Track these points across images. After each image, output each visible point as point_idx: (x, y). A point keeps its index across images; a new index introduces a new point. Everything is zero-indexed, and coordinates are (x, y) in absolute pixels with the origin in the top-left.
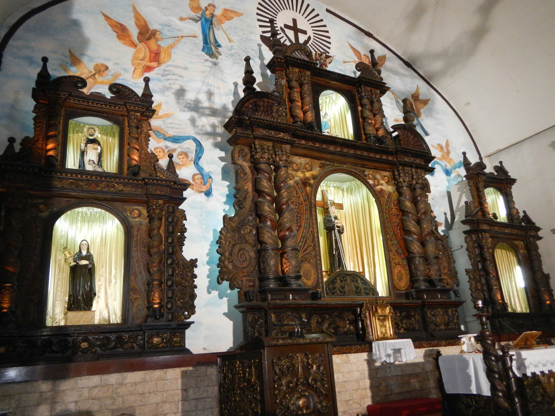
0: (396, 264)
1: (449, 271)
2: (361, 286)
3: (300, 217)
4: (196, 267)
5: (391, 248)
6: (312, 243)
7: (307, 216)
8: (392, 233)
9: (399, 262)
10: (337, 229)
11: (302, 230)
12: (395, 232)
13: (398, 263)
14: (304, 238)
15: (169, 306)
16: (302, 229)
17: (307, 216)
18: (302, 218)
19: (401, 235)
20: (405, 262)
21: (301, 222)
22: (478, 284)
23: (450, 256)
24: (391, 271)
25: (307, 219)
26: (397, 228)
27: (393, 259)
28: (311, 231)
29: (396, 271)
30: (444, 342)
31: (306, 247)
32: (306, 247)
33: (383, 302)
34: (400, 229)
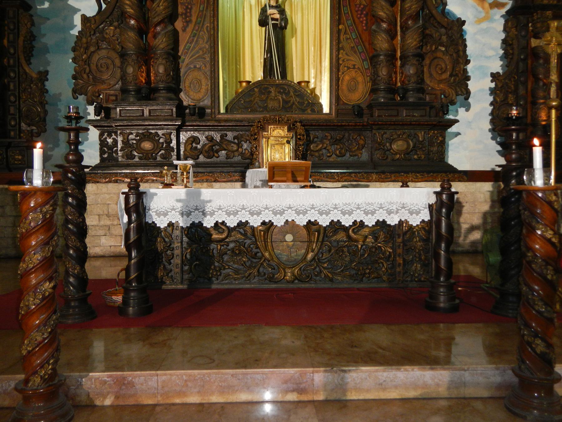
0: (349, 68)
1: (451, 76)
2: (294, 99)
3: (191, 9)
4: (47, 80)
5: (344, 44)
6: (207, 43)
7: (202, 6)
8: (349, 22)
9: (354, 65)
10: (271, 22)
11: (193, 26)
12: (356, 19)
13: (352, 67)
14: (194, 36)
15: (13, 123)
16: (191, 27)
17: (202, 6)
18: (193, 11)
19: (366, 24)
20: (366, 65)
21: (191, 16)
22: (510, 95)
23: (461, 53)
24: (338, 80)
25: (203, 11)
26: (361, 14)
27: (343, 61)
28: (207, 26)
29: (347, 78)
30: (374, 176)
31: (197, 49)
32: (197, 49)
33: (288, 120)
34: (366, 15)
